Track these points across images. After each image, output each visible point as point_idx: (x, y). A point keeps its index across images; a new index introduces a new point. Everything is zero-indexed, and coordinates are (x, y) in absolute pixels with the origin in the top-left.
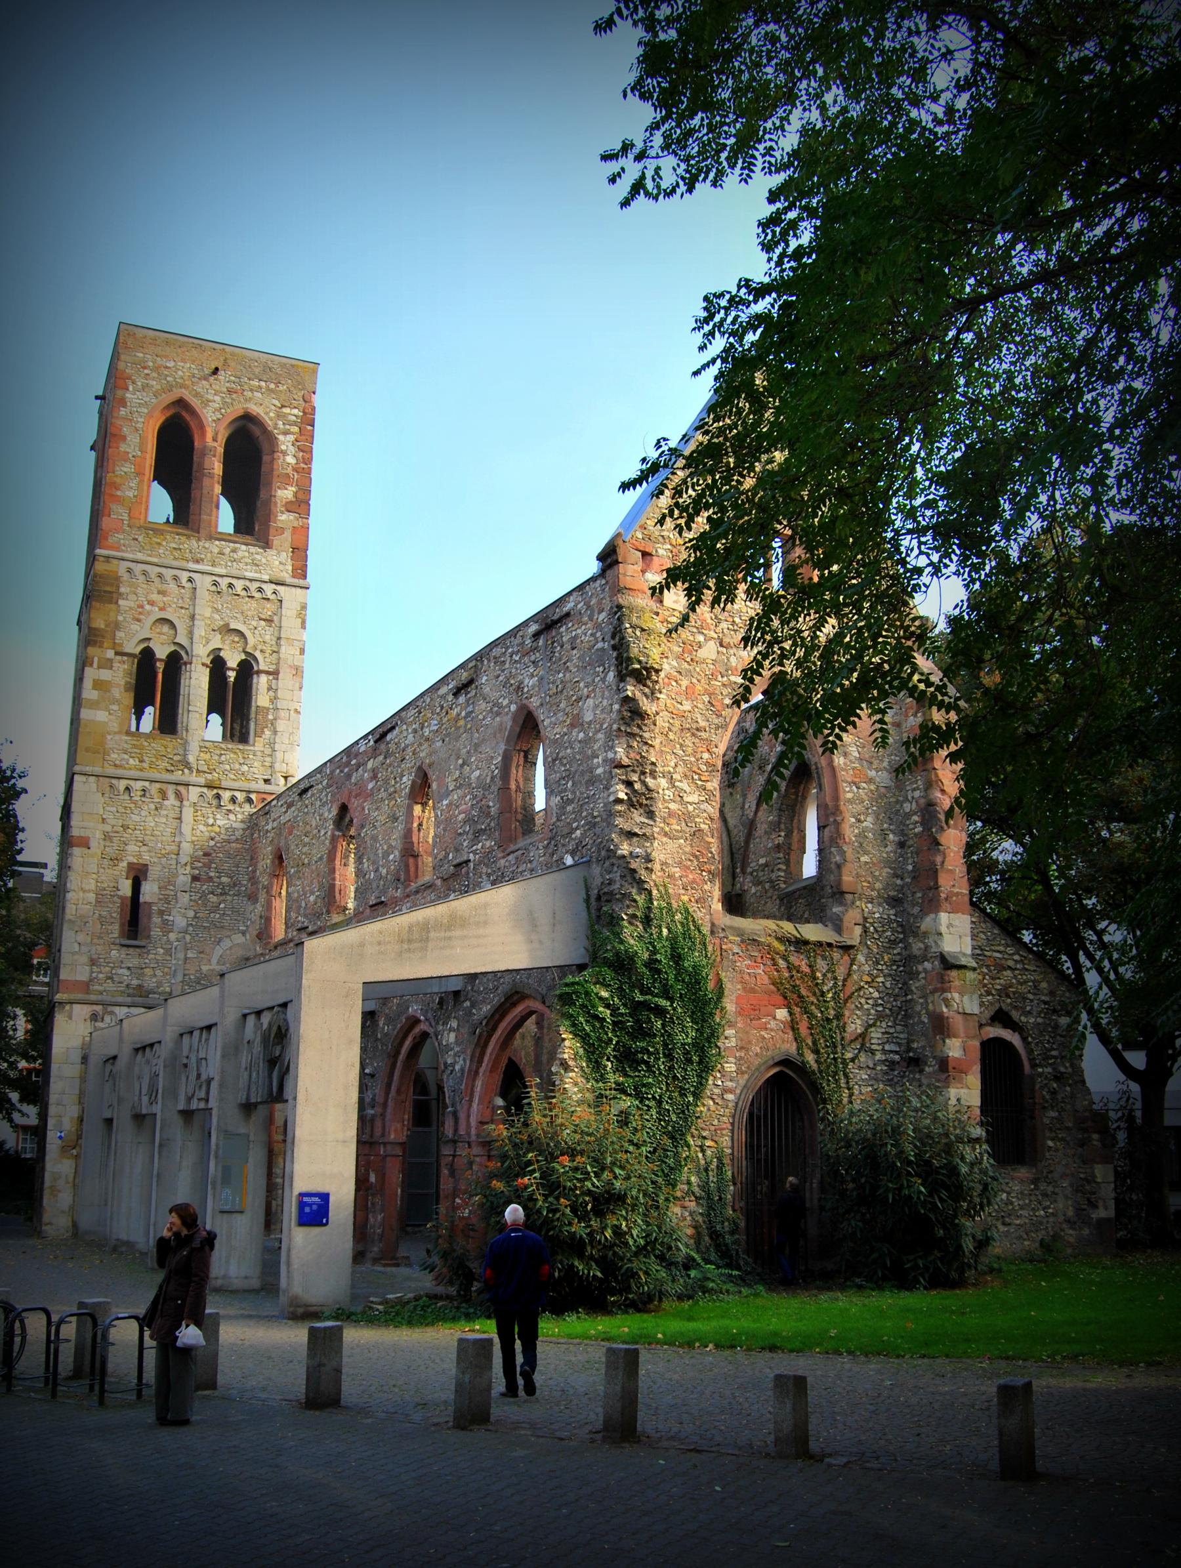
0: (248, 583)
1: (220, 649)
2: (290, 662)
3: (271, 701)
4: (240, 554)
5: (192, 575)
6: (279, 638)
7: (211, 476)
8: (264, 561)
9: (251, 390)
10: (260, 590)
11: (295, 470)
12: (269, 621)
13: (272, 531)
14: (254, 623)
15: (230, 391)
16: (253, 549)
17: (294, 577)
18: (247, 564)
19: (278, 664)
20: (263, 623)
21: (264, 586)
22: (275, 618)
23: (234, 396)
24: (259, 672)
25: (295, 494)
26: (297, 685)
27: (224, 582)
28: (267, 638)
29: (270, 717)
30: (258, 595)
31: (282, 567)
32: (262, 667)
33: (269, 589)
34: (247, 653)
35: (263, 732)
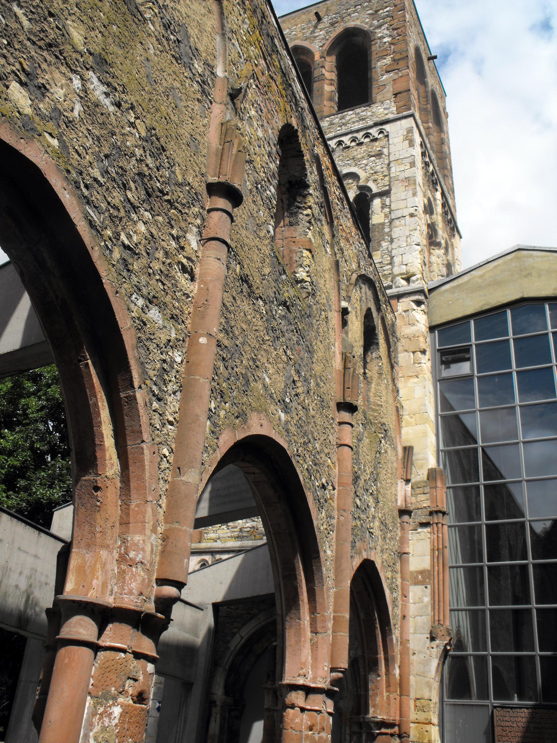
4: (348, 118)
6: (389, 165)
7: (322, 78)
8: (369, 114)
9: (349, 15)
10: (367, 135)
11: (391, 44)
12: (379, 155)
13: (374, 91)
14: (365, 162)
15: (332, 24)
16: (358, 111)
18: (354, 122)
19: (389, 185)
21: (370, 131)
22: (385, 151)
23: (336, 25)
25: (394, 60)
26: (410, 193)
28: (378, 168)
29: (387, 230)
30: (367, 140)
31: (386, 112)
33: (374, 132)
34: (360, 188)
35: (380, 245)
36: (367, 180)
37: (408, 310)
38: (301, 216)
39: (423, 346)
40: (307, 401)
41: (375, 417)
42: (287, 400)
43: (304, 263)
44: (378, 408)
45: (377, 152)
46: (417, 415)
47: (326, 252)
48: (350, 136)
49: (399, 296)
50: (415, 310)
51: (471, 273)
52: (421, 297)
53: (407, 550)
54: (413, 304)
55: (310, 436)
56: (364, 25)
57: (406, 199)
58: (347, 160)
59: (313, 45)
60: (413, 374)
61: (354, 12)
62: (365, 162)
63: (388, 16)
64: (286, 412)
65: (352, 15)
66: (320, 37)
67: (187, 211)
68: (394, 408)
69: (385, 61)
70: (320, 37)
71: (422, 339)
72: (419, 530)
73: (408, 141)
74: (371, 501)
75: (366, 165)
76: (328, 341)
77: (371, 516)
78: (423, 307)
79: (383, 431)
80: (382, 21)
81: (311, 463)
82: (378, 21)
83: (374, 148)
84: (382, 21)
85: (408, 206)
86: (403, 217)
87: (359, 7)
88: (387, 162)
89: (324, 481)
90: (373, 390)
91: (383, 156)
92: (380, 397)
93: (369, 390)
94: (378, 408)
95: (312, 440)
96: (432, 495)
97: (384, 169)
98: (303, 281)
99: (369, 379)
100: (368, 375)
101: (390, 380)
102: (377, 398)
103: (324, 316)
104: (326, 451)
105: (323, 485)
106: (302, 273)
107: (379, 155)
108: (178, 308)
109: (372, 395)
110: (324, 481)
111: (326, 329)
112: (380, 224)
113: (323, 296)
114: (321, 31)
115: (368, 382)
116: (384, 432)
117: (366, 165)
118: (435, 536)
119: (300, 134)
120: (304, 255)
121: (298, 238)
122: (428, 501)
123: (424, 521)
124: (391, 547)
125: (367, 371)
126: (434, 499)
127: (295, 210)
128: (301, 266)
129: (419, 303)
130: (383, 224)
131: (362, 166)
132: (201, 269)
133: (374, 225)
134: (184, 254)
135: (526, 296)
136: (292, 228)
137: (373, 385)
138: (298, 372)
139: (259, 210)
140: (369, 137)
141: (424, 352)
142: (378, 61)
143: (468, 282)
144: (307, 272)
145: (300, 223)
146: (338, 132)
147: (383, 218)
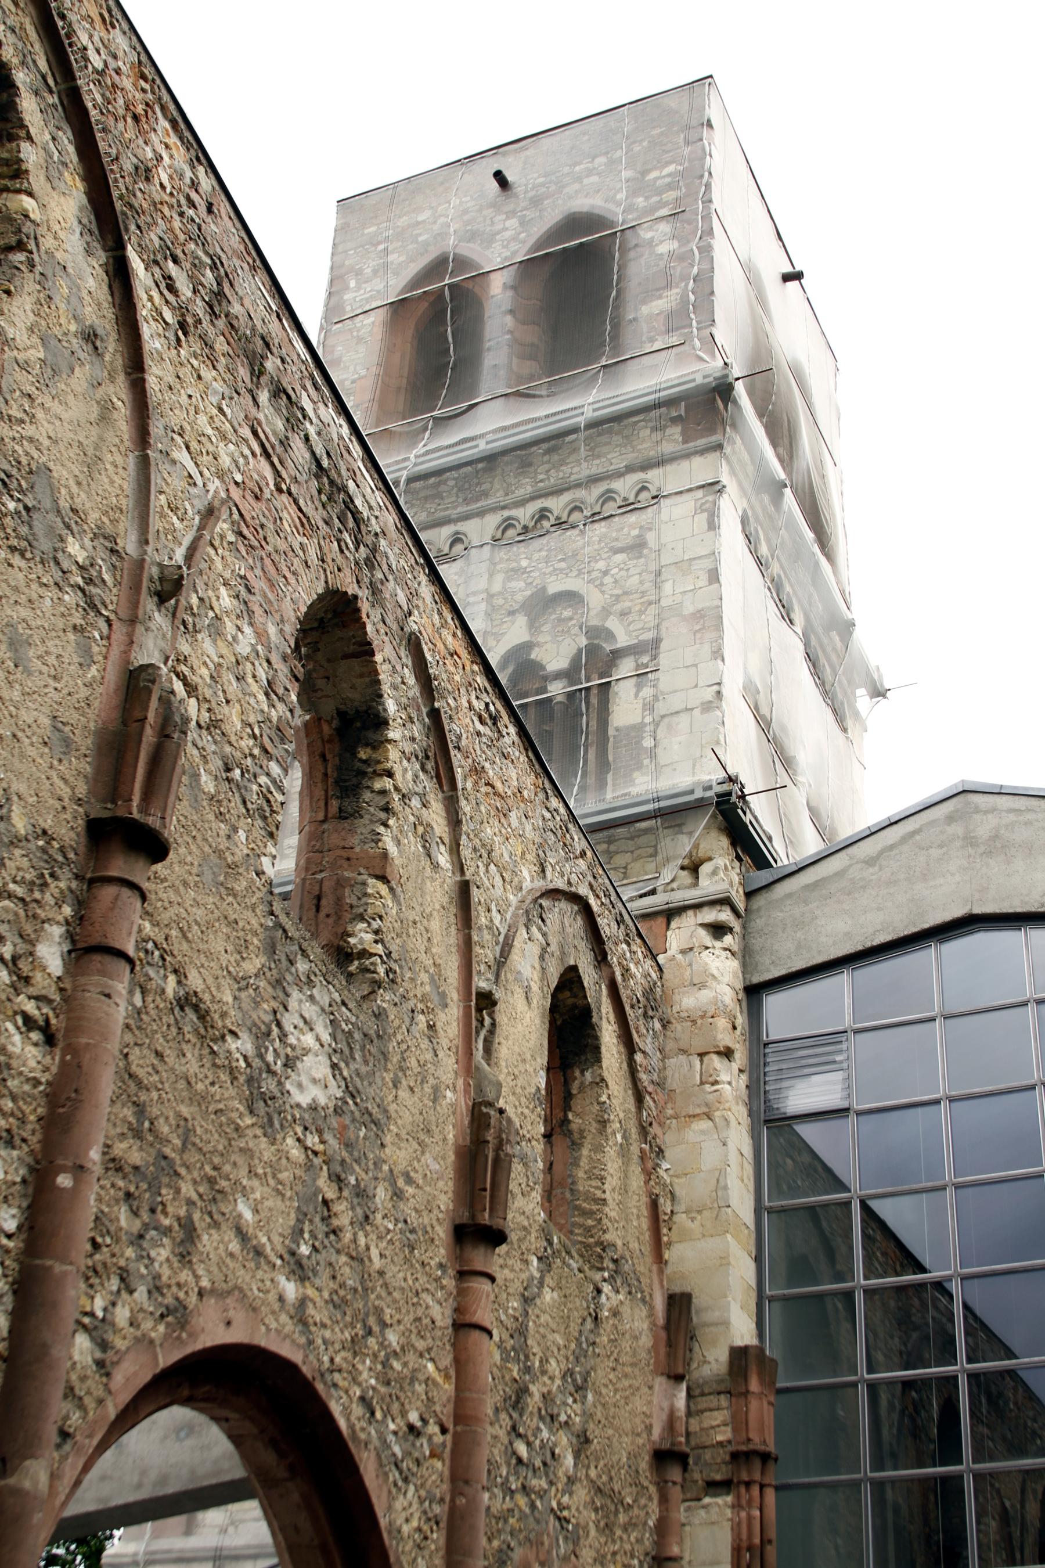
0: (581, 493)
1: (528, 646)
2: (689, 608)
3: (649, 707)
5: (461, 527)
6: (658, 574)
9: (579, 180)
12: (637, 547)
14: (601, 565)
17: (685, 442)
20: (620, 557)
21: (617, 485)
22: (650, 537)
24: (616, 655)
26: (706, 650)
27: (524, 514)
29: (648, 743)
32: (623, 640)
36: (606, 612)
37: (691, 949)
38: (367, 796)
39: (725, 1038)
40: (362, 1241)
41: (588, 1229)
42: (304, 1250)
43: (370, 911)
44: (594, 1207)
45: (629, 541)
46: (706, 1214)
47: (436, 866)
48: (567, 497)
49: (671, 914)
50: (707, 948)
51: (850, 850)
52: (725, 915)
53: (675, 1550)
54: (702, 933)
55: (372, 1321)
56: (611, 206)
57: (696, 665)
58: (560, 561)
59: (488, 253)
60: (698, 1111)
61: (590, 172)
62: (601, 565)
63: (670, 187)
64: (303, 1279)
65: (586, 181)
66: (507, 234)
67: (37, 895)
68: (645, 1199)
69: (660, 302)
70: (507, 234)
71: (722, 1023)
72: (707, 1500)
73: (705, 514)
74: (564, 1441)
75: (606, 573)
76: (432, 1081)
77: (565, 1480)
78: (728, 939)
79: (607, 1263)
80: (655, 199)
81: (373, 1382)
82: (647, 198)
83: (626, 530)
84: (655, 199)
85: (701, 683)
86: (687, 709)
87: (602, 160)
88: (652, 567)
89: (414, 1417)
90: (584, 1162)
91: (645, 551)
92: (602, 1179)
93: (576, 1164)
94: (594, 1207)
95: (376, 1329)
96: (734, 1416)
97: (648, 585)
98: (364, 954)
99: (576, 1136)
100: (574, 1127)
101: (634, 1130)
102: (594, 1183)
103: (423, 1026)
104: (421, 1345)
105: (411, 1428)
106: (363, 935)
107: (637, 547)
108: (12, 1114)
109: (581, 1174)
110: (414, 1417)
111: (429, 1056)
112: (633, 727)
113: (424, 977)
114: (508, 218)
115: (573, 1143)
116: (611, 1266)
117: (606, 573)
118: (743, 1514)
119: (365, 606)
120: (370, 891)
121: (357, 849)
122: (729, 1429)
123: (718, 1477)
124: (628, 1547)
125: (570, 1116)
126: (739, 1422)
127: (354, 781)
128: (361, 918)
129: (718, 930)
130: (639, 728)
131: (595, 574)
132: (69, 1019)
133: (617, 729)
134: (31, 991)
135: (977, 910)
136: (346, 824)
137: (585, 1152)
138: (338, 1180)
139: (235, 830)
140: (615, 500)
141: (727, 1054)
142: (644, 302)
143: (840, 874)
144: (377, 932)
145: (363, 812)
146: (541, 485)
147: (639, 711)
